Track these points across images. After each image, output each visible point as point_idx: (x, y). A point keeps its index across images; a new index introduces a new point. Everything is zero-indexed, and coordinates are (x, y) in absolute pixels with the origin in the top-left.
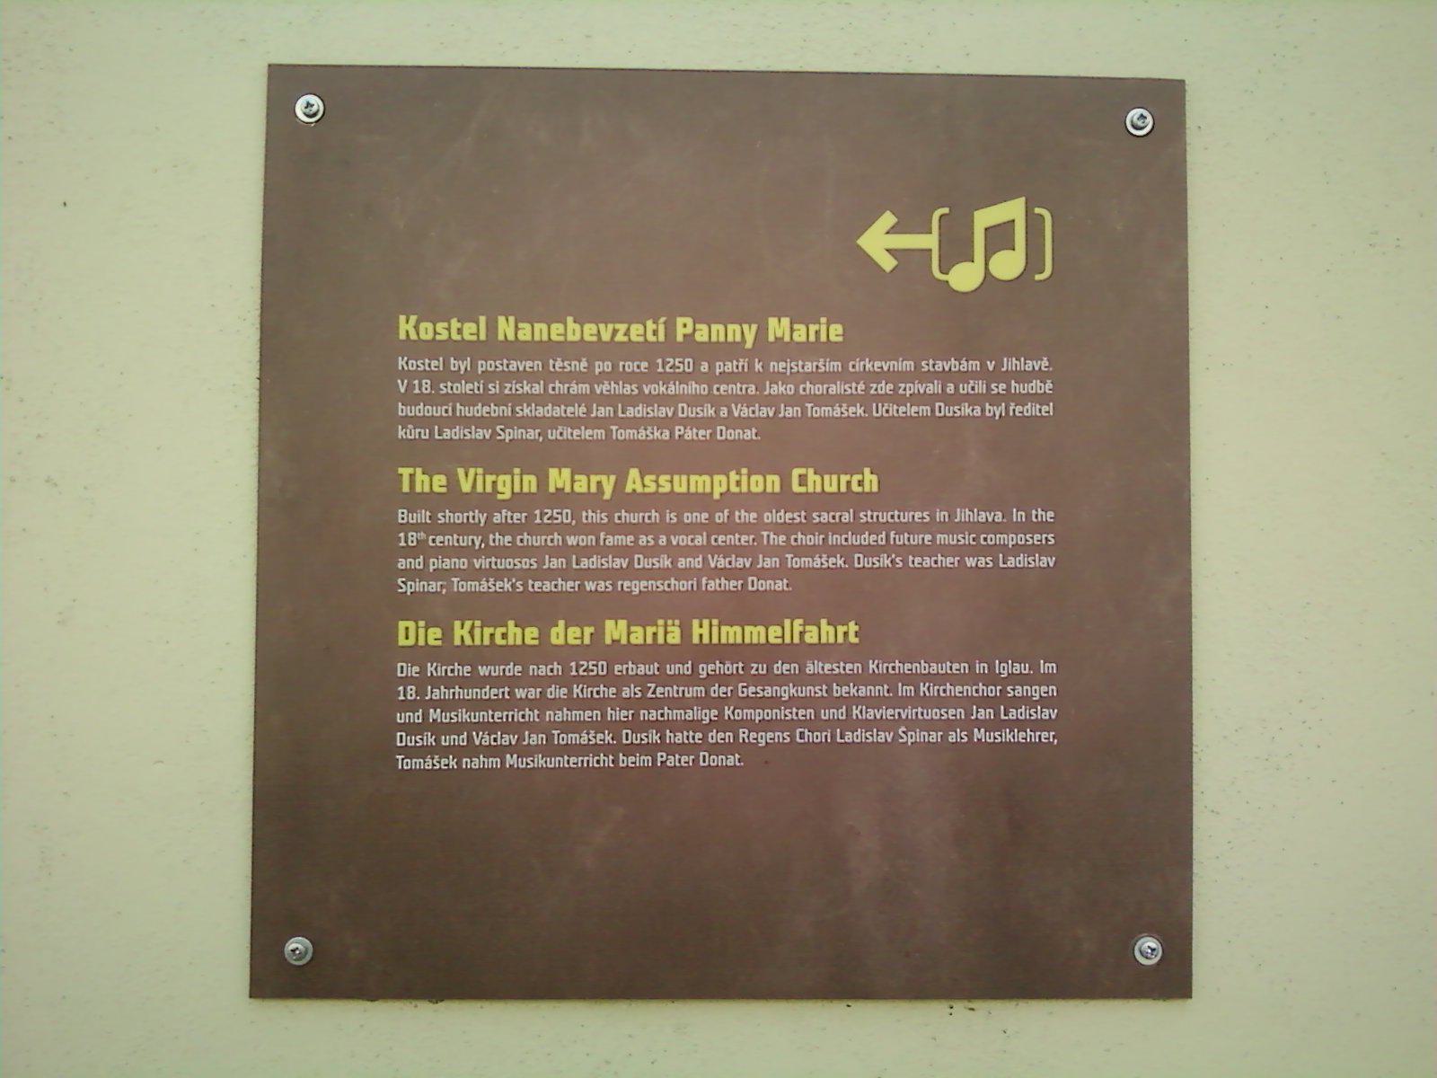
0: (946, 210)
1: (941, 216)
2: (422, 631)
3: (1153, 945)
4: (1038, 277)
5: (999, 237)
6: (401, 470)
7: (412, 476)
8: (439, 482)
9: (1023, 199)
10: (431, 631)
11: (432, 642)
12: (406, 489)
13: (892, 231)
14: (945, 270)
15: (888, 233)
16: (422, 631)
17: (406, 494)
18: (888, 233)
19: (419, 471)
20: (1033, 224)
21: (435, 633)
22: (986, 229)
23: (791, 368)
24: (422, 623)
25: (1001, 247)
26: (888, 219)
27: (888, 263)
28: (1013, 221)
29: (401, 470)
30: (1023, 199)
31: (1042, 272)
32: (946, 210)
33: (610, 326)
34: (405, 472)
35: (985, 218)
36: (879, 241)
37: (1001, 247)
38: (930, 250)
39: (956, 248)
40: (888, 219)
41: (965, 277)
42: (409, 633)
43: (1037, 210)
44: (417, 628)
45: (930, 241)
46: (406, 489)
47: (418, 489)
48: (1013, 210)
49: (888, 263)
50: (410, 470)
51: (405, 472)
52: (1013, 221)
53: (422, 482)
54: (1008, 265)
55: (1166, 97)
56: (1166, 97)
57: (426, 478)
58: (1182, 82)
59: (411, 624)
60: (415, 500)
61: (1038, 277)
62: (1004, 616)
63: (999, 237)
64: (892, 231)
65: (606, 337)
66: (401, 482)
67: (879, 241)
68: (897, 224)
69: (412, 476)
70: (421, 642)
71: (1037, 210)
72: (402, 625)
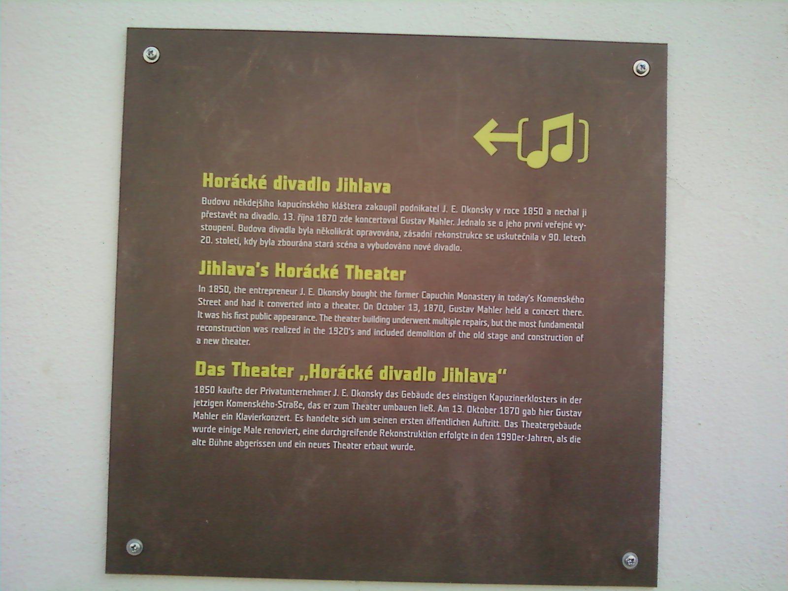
0: (526, 120)
1: (524, 123)
4: (580, 161)
5: (558, 136)
9: (572, 114)
14: (525, 155)
15: (492, 132)
18: (492, 132)
22: (550, 131)
25: (558, 142)
26: (492, 124)
27: (491, 150)
28: (566, 126)
30: (572, 114)
32: (526, 120)
35: (550, 125)
36: (487, 137)
38: (517, 143)
39: (532, 142)
40: (492, 124)
41: (536, 160)
43: (581, 121)
45: (516, 138)
48: (566, 120)
49: (491, 150)
52: (566, 126)
54: (563, 153)
55: (657, 53)
56: (657, 53)
58: (665, 46)
61: (580, 161)
63: (558, 136)
67: (487, 137)
71: (581, 121)
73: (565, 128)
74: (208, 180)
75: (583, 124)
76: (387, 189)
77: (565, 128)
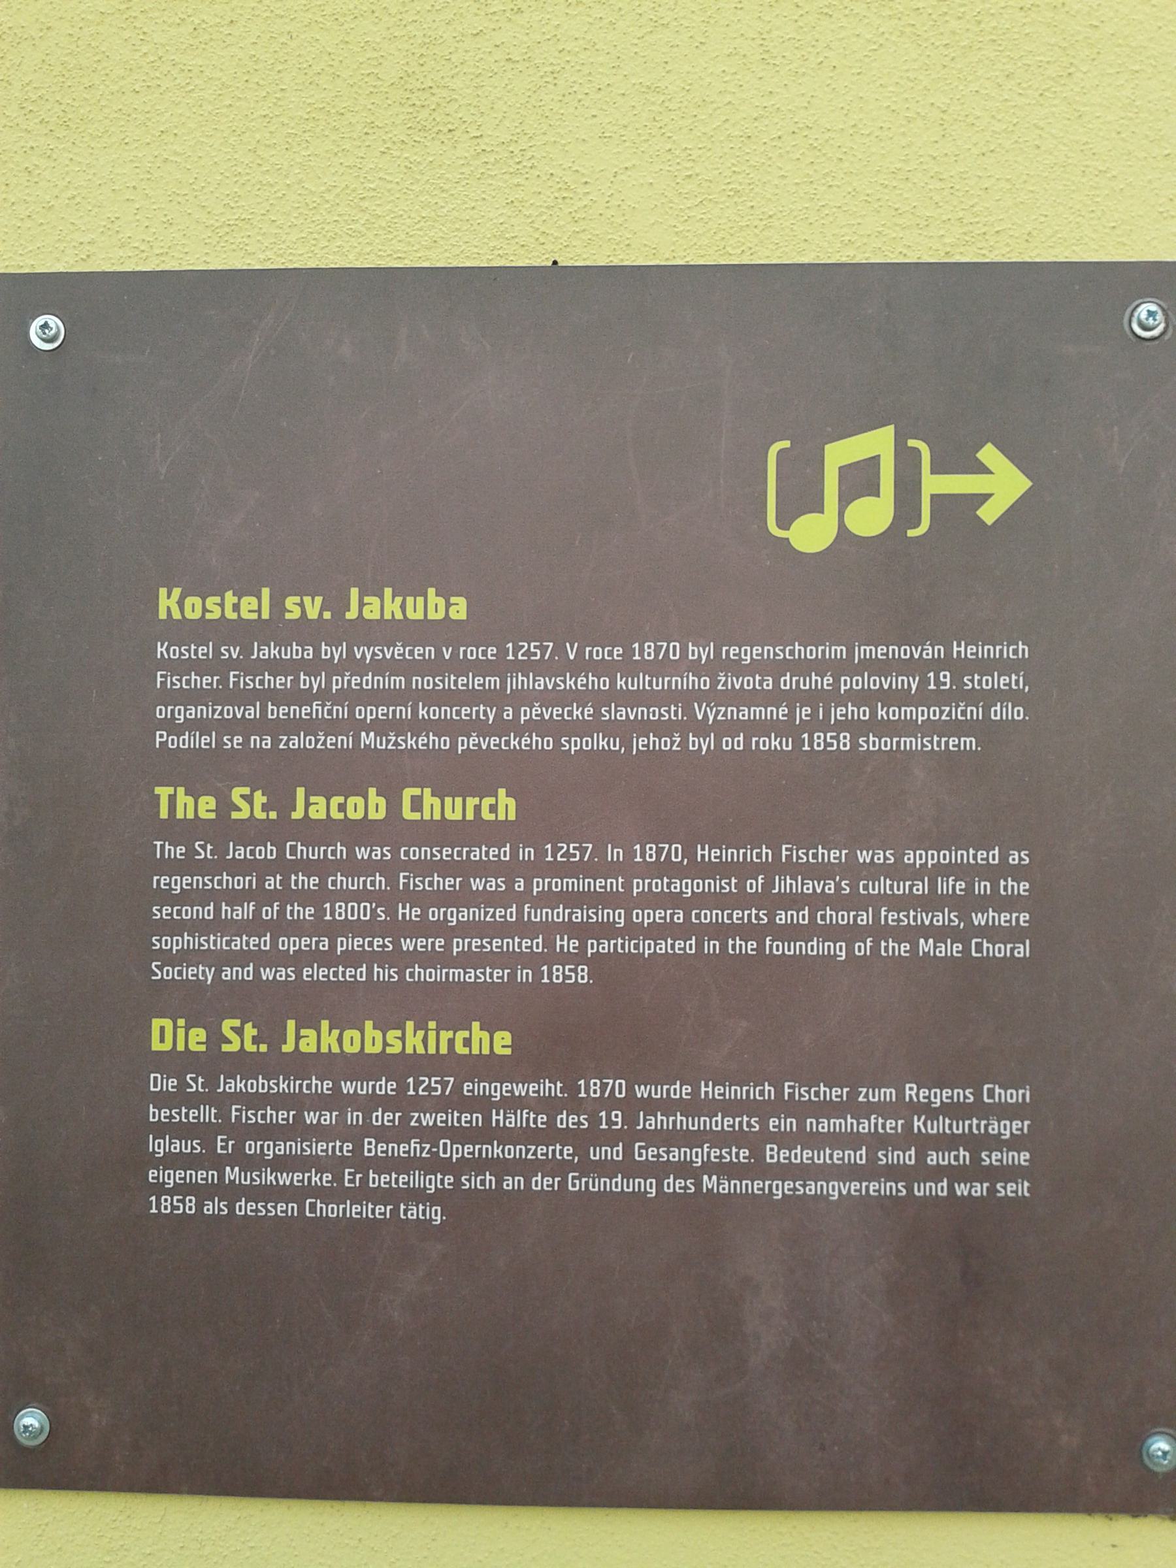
5: (860, 480)
6: (158, 790)
7: (172, 799)
8: (207, 806)
9: (891, 428)
12: (164, 814)
14: (784, 524)
19: (181, 791)
22: (840, 468)
29: (158, 790)
30: (891, 428)
34: (163, 792)
35: (839, 454)
41: (811, 534)
43: (912, 443)
46: (164, 814)
47: (180, 815)
48: (878, 443)
50: (171, 790)
51: (163, 792)
63: (860, 480)
69: (172, 799)
71: (912, 443)
73: (875, 460)
75: (917, 452)
76: (460, 609)
77: (875, 460)
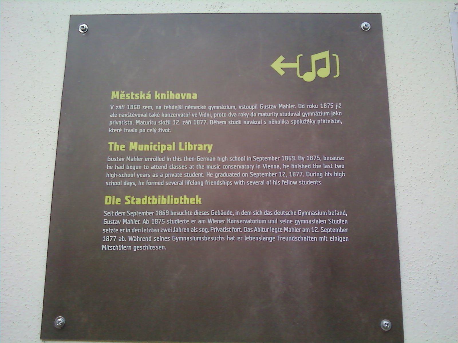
0: (301, 55)
2: (114, 199)
3: (387, 322)
4: (335, 77)
5: (321, 64)
6: (109, 143)
7: (113, 145)
8: (123, 147)
9: (328, 51)
10: (117, 199)
11: (117, 203)
12: (111, 149)
13: (283, 62)
14: (302, 74)
16: (114, 199)
17: (111, 151)
18: (281, 63)
19: (116, 143)
20: (332, 60)
21: (118, 200)
22: (316, 61)
23: (179, 108)
24: (114, 197)
25: (321, 66)
26: (281, 58)
27: (282, 73)
28: (325, 58)
29: (109, 143)
30: (328, 51)
31: (336, 74)
32: (301, 55)
33: (185, 94)
34: (111, 144)
35: (315, 57)
36: (278, 65)
37: (321, 66)
39: (306, 67)
40: (281, 58)
41: (309, 77)
42: (109, 200)
43: (333, 55)
44: (112, 198)
46: (111, 149)
47: (115, 150)
48: (325, 55)
49: (282, 73)
50: (113, 143)
51: (111, 144)
52: (325, 58)
53: (117, 147)
54: (324, 73)
57: (118, 146)
59: (110, 197)
60: (114, 154)
61: (335, 77)
62: (329, 195)
63: (321, 64)
64: (283, 62)
65: (183, 98)
66: (109, 147)
67: (278, 65)
68: (285, 59)
69: (113, 145)
70: (113, 203)
71: (333, 55)
72: (107, 197)
74: (115, 95)
